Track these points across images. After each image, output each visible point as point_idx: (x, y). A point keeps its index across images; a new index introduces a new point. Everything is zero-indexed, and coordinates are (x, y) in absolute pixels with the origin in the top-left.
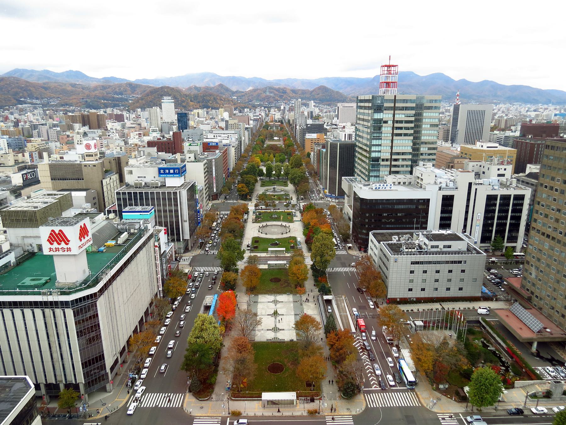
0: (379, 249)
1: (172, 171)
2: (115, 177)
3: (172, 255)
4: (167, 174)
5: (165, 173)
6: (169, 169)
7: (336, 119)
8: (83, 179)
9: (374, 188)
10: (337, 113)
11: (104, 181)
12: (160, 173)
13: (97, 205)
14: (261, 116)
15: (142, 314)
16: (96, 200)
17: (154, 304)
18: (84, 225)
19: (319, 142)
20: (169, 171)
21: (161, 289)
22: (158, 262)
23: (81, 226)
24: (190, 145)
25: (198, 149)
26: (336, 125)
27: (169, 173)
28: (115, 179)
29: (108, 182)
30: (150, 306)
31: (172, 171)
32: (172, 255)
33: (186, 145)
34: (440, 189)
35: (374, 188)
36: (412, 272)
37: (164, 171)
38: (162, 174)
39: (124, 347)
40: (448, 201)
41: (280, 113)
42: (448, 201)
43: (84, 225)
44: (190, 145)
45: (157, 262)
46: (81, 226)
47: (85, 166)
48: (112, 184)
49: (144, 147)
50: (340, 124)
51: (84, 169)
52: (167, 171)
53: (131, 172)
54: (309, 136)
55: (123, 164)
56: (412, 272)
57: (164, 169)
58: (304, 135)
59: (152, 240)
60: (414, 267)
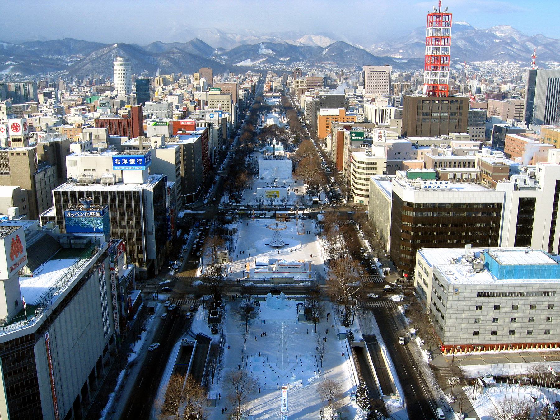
0: (431, 275)
1: (132, 161)
2: (51, 170)
3: (132, 282)
4: (124, 165)
5: (122, 165)
6: (128, 159)
7: (360, 88)
8: (8, 173)
9: (422, 187)
10: (361, 79)
11: (37, 176)
12: (115, 165)
13: (27, 211)
14: (253, 84)
15: (93, 365)
16: (26, 203)
17: (108, 351)
18: (17, 236)
19: (339, 120)
20: (128, 161)
21: (118, 330)
22: (115, 292)
23: (13, 239)
24: (156, 125)
25: (165, 131)
26: (361, 97)
27: (128, 164)
28: (51, 173)
29: (43, 177)
30: (104, 355)
31: (132, 161)
32: (132, 282)
33: (148, 124)
34: (516, 188)
35: (422, 187)
36: (478, 308)
37: (121, 161)
38: (118, 165)
39: (70, 411)
40: (527, 207)
41: (280, 79)
42: (527, 207)
43: (17, 236)
44: (156, 125)
45: (113, 292)
46: (13, 239)
47: (12, 154)
48: (47, 180)
49: (91, 127)
50: (368, 95)
51: (11, 159)
52: (125, 161)
53: (75, 163)
54: (323, 112)
55: (63, 152)
56: (478, 308)
57: (121, 159)
58: (317, 110)
59: (107, 260)
60: (481, 301)
